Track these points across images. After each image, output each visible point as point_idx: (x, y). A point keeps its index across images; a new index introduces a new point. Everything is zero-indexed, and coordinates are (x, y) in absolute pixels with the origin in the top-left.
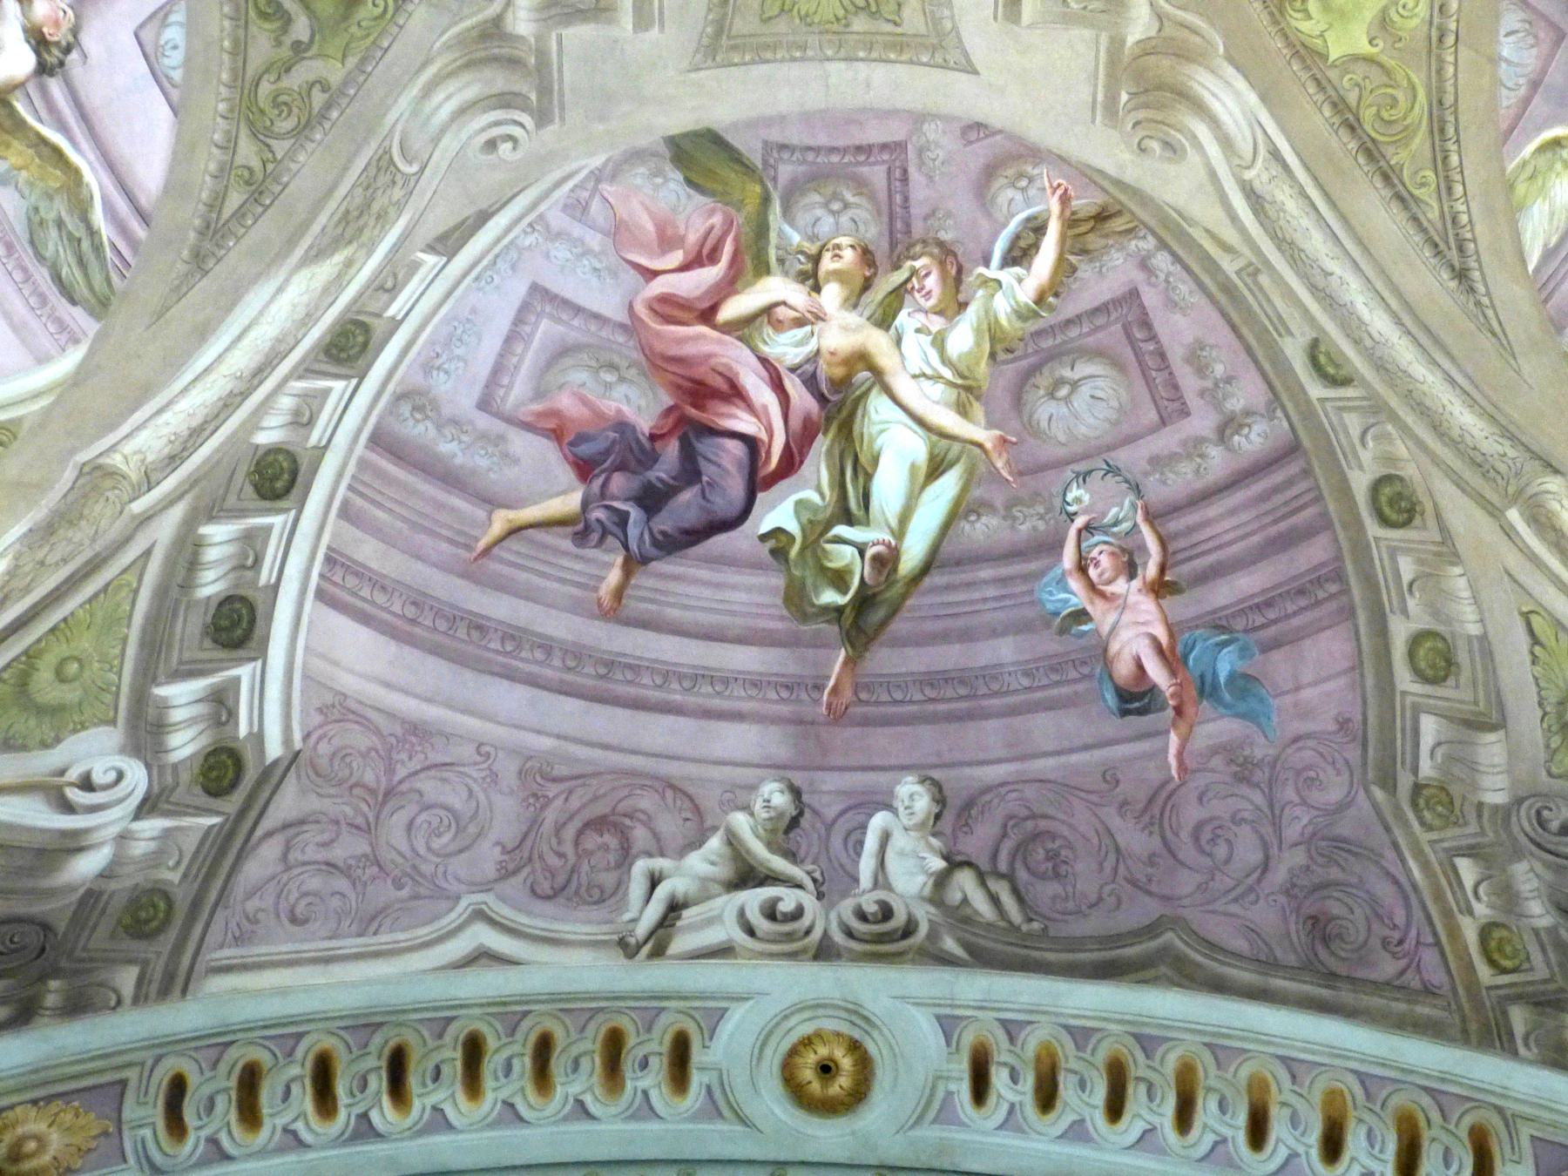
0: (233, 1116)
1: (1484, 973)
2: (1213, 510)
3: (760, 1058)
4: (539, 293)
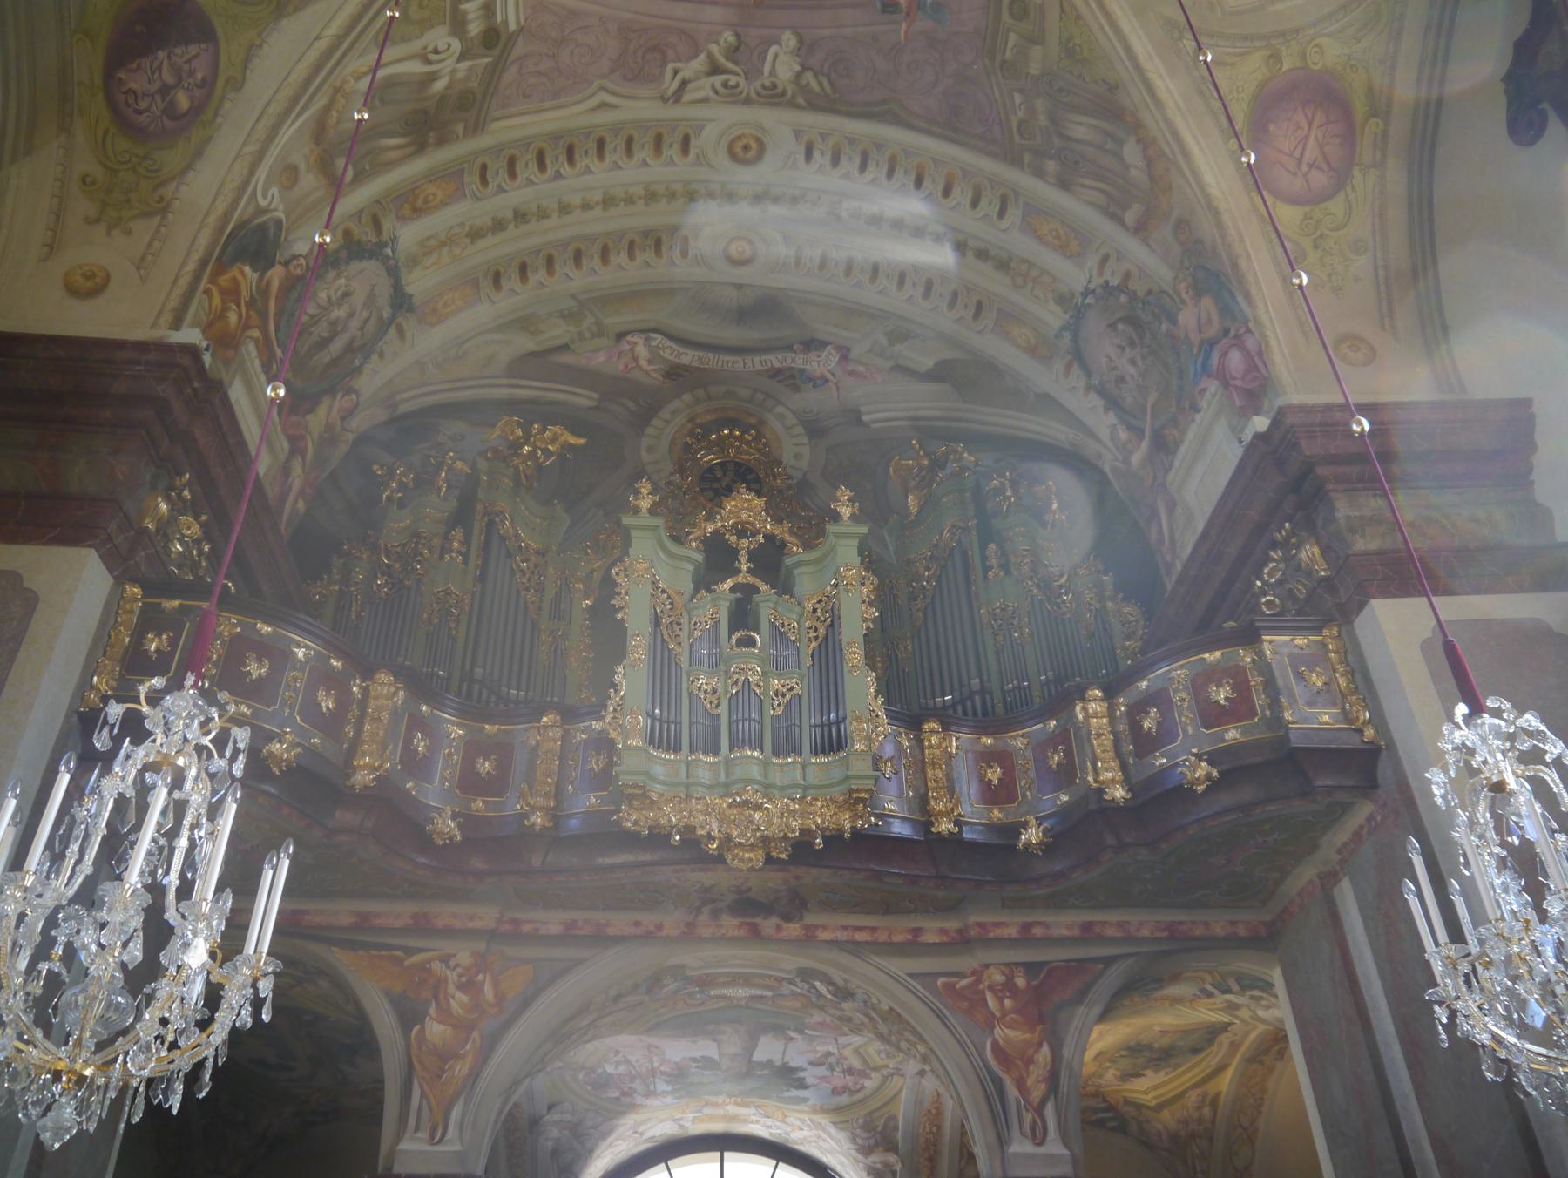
0: (506, 176)
1: (1017, 138)
3: (719, 143)
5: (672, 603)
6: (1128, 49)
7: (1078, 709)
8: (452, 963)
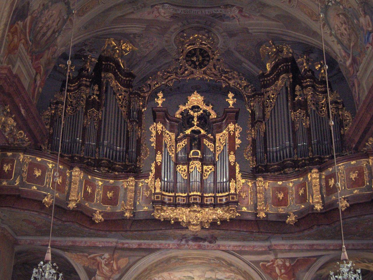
5: (170, 138)
7: (309, 176)
8: (103, 257)
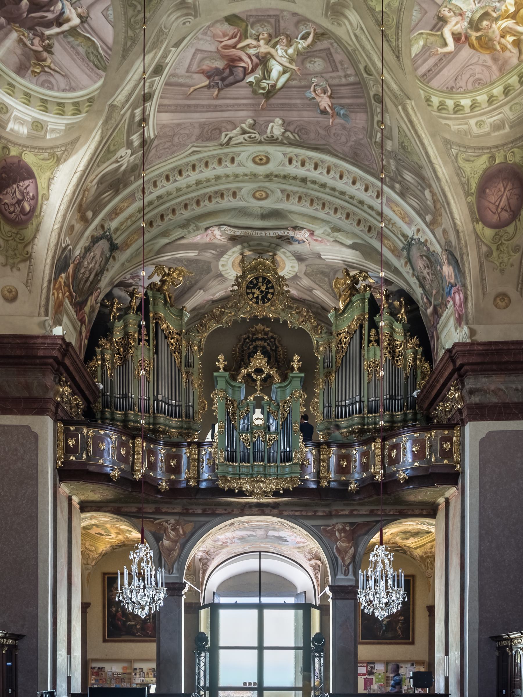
2: (342, 88)
4: (197, 50)
6: (427, 153)
